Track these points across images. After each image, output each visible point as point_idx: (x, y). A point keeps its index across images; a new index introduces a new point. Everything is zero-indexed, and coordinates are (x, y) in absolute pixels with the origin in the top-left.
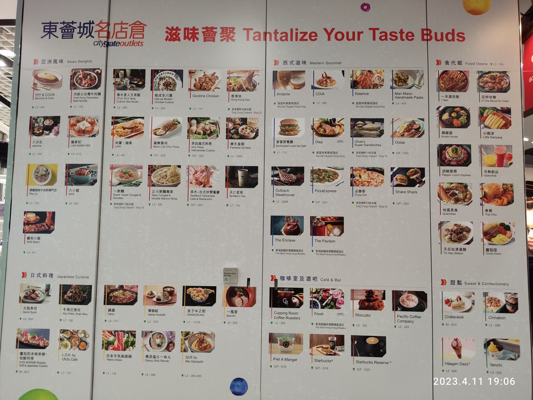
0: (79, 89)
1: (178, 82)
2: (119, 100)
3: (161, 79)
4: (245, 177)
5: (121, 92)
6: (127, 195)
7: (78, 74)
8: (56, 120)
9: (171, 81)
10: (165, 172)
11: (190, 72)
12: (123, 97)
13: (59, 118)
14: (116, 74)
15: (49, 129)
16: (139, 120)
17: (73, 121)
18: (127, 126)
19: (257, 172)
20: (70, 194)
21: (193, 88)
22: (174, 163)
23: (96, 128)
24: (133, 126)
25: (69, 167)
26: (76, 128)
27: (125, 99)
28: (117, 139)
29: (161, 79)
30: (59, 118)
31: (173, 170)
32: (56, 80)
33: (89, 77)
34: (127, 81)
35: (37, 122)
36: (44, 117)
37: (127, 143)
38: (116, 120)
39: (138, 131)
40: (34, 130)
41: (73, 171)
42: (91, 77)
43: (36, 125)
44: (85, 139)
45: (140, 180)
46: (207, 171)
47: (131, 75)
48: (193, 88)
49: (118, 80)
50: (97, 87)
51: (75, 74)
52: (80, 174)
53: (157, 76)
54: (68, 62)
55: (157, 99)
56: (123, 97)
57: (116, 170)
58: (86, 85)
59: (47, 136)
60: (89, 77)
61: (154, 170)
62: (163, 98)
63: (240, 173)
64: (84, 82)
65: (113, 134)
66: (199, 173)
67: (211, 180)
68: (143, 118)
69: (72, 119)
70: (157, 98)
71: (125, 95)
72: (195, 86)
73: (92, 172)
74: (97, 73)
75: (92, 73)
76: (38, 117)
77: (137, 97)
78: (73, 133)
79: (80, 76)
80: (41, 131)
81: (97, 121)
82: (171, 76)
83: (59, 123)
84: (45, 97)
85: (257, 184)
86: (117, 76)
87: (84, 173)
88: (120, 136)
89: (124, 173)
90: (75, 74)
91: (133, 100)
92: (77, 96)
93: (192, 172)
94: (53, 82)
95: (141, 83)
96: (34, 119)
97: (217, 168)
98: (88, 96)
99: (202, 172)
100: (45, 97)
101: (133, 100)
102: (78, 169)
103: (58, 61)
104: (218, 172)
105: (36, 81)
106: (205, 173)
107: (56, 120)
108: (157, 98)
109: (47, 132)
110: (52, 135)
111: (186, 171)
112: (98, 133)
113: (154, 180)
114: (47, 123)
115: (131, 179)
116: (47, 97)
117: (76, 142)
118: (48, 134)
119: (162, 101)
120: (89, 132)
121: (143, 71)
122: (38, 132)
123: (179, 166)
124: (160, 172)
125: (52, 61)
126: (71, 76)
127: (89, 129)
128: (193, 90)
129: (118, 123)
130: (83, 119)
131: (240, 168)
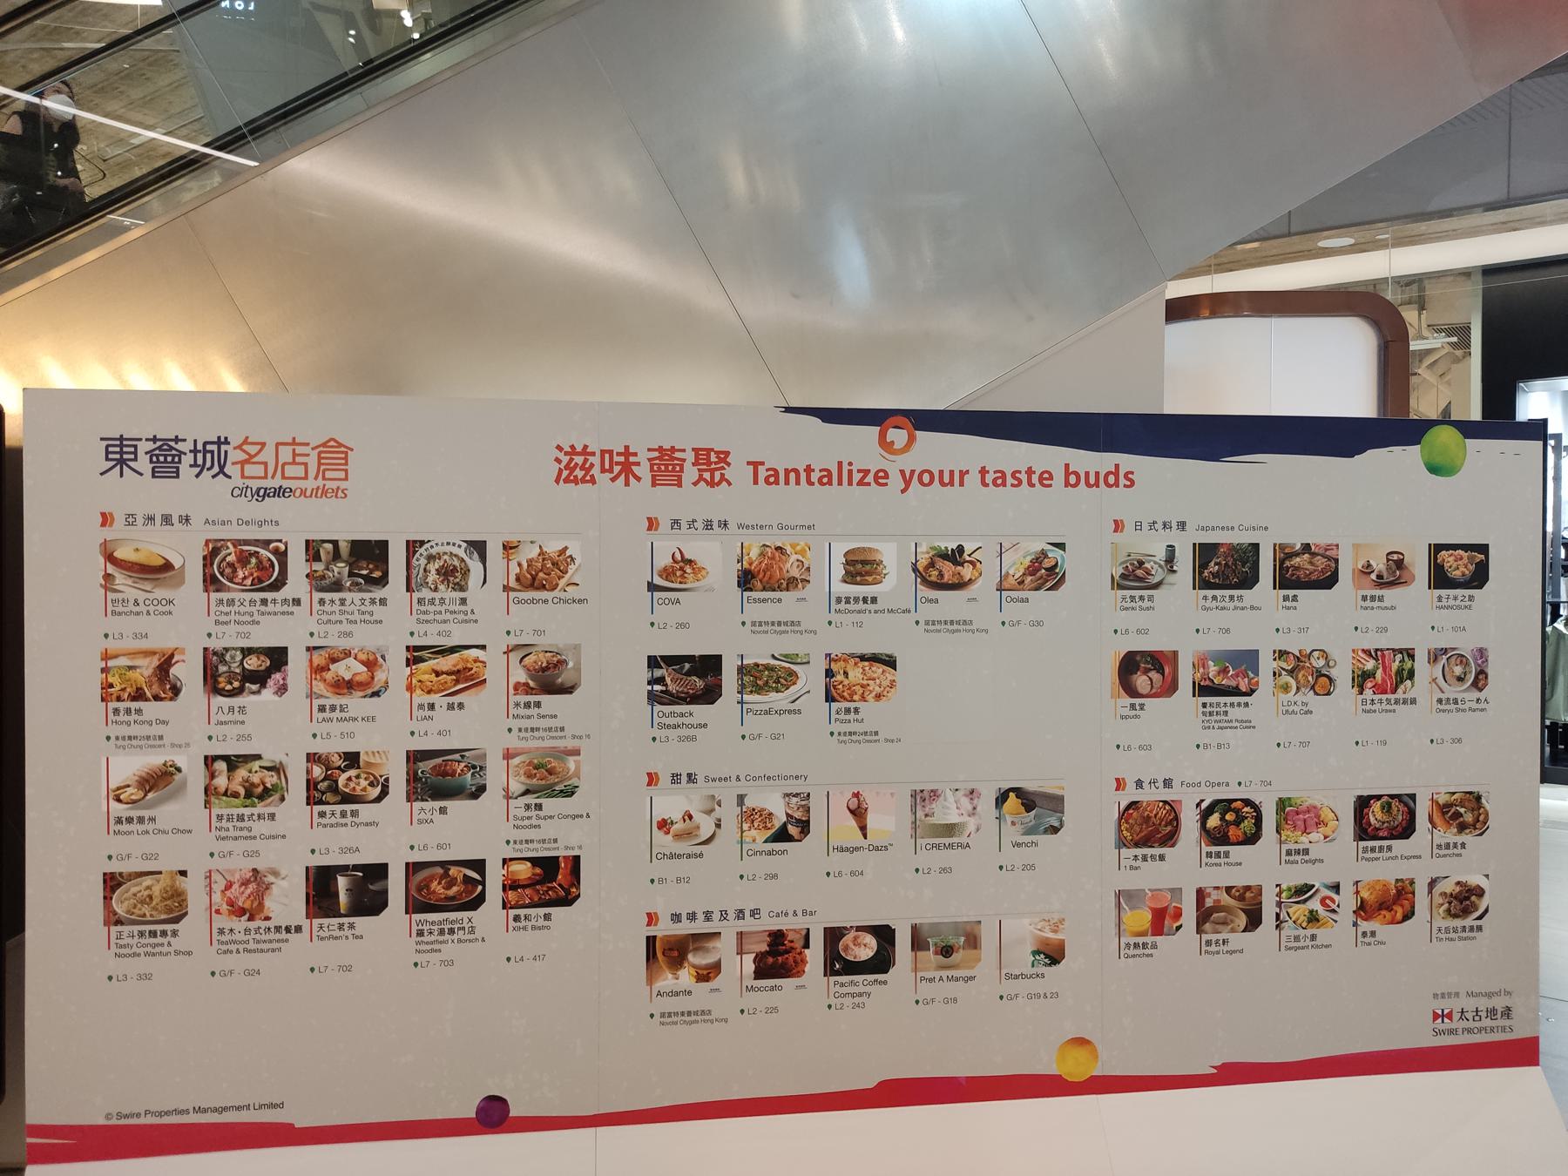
0: (229, 590)
1: (475, 565)
2: (325, 618)
3: (431, 558)
4: (356, 891)
5: (327, 596)
6: (551, 817)
7: (224, 553)
8: (278, 657)
9: (456, 563)
10: (149, 888)
11: (505, 547)
12: (336, 608)
13: (284, 651)
14: (311, 552)
15: (259, 678)
16: (474, 653)
17: (318, 659)
18: (445, 669)
19: (386, 877)
20: (420, 822)
21: (513, 583)
22: (167, 864)
23: (380, 676)
24: (460, 667)
25: (414, 757)
26: (329, 676)
27: (342, 613)
28: (420, 698)
29: (431, 558)
30: (284, 651)
31: (169, 882)
32: (167, 566)
33: (254, 560)
34: (341, 568)
35: (223, 661)
36: (242, 650)
37: (451, 707)
38: (415, 655)
39: (476, 675)
40: (216, 682)
41: (425, 766)
42: (260, 562)
43: (222, 669)
44: (356, 704)
45: (574, 781)
46: (258, 881)
47: (351, 555)
48: (513, 583)
49: (319, 567)
50: (278, 585)
51: (215, 552)
52: (445, 774)
53: (422, 550)
54: (207, 521)
55: (425, 613)
56: (336, 608)
57: (516, 761)
58: (249, 582)
59: (253, 698)
60: (254, 560)
61: (120, 885)
62: (443, 609)
63: (342, 882)
64: (241, 574)
65: (410, 688)
66: (236, 886)
67: (268, 903)
68: (483, 647)
69: (316, 654)
70: (423, 608)
71: (342, 602)
72: (518, 579)
73: (474, 767)
74: (276, 552)
75: (262, 552)
76: (227, 650)
77: (376, 608)
78: (319, 687)
79: (229, 559)
80: (236, 684)
81: (383, 657)
82: (455, 550)
83: (286, 663)
84: (142, 608)
85: (385, 905)
86: (317, 558)
87: (454, 772)
88: (429, 692)
89: (536, 768)
90: (215, 552)
91: (367, 617)
92: (226, 609)
93: (219, 886)
94: (158, 571)
95: (377, 574)
96: (215, 653)
97: (283, 873)
98: (263, 608)
99: (245, 883)
100: (142, 608)
101: (367, 617)
102: (439, 761)
103: (175, 520)
104: (284, 884)
105: (111, 569)
106: (252, 887)
107: (278, 657)
108: (423, 608)
109: (254, 687)
110: (268, 694)
111: (203, 883)
112: (386, 686)
113: (120, 910)
114: (252, 663)
115: (552, 779)
116: (152, 608)
117: (333, 708)
118: (258, 692)
119: (438, 617)
120: (362, 686)
121: (383, 545)
122: (229, 687)
123: (183, 873)
124: (134, 890)
125: (158, 520)
126: (205, 558)
127: (363, 678)
128: (514, 590)
129: (422, 660)
130: (347, 654)
131: (343, 869)
